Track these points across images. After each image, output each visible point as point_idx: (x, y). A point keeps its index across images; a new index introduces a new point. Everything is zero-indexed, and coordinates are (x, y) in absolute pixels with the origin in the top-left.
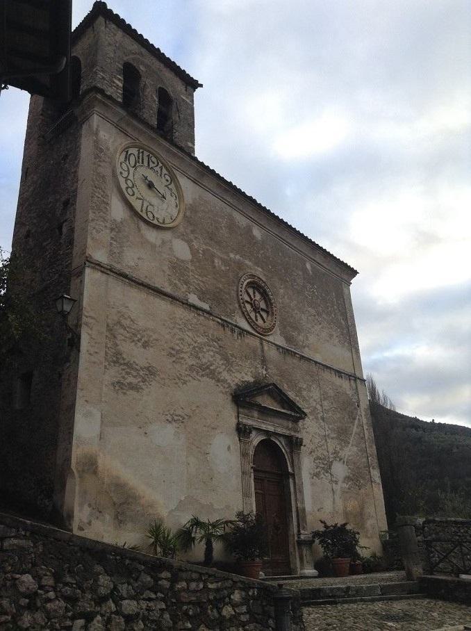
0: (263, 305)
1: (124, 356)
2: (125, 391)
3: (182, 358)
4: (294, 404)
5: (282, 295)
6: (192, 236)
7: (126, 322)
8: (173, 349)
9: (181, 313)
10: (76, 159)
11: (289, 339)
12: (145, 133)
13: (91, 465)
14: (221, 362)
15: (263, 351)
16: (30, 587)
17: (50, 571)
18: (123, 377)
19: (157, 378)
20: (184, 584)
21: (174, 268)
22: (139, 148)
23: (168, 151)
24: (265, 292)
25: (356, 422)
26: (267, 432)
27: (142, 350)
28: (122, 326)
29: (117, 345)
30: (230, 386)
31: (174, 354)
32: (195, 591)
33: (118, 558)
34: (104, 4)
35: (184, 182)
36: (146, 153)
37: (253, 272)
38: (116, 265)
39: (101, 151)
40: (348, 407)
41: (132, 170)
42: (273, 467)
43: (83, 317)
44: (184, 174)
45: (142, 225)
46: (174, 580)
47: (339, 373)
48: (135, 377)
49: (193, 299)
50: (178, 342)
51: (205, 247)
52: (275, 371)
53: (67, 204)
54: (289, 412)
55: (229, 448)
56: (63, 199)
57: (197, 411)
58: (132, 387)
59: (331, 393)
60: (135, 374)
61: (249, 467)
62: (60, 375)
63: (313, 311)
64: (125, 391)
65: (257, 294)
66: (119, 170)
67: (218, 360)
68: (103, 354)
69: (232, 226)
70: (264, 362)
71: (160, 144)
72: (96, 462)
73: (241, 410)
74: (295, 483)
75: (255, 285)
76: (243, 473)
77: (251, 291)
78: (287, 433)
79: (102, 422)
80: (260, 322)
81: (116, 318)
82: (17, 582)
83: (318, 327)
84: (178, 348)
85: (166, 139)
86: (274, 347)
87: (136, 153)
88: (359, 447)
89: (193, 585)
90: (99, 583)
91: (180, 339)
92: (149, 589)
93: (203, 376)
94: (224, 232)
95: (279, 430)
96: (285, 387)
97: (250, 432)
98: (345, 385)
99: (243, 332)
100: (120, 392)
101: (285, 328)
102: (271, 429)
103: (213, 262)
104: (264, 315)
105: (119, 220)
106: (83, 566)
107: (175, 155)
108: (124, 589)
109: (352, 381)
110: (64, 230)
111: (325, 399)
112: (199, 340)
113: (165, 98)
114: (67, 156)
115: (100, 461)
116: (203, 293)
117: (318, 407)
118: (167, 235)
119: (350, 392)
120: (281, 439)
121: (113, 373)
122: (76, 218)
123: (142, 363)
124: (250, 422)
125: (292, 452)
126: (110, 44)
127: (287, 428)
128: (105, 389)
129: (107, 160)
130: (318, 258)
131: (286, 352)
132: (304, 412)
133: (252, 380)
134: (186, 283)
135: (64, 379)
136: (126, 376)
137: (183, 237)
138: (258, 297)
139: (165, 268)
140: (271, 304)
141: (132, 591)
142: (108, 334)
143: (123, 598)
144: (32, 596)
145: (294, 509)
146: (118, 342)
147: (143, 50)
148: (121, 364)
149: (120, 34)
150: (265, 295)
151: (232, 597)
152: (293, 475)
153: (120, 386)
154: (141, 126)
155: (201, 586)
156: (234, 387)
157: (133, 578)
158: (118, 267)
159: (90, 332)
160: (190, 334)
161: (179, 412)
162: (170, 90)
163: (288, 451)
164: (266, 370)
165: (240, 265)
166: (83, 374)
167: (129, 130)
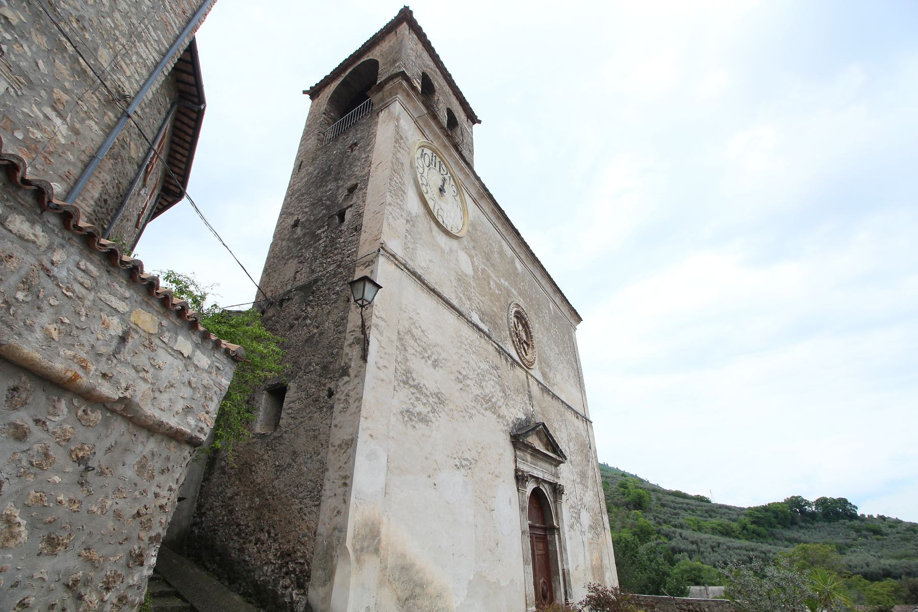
1: (414, 375)
2: (413, 423)
3: (468, 386)
6: (473, 252)
7: (417, 332)
10: (369, 145)
12: (439, 137)
13: (372, 538)
18: (413, 404)
19: (446, 409)
21: (460, 280)
22: (434, 151)
23: (457, 163)
24: (526, 323)
27: (432, 369)
28: (413, 336)
30: (508, 424)
31: (461, 379)
34: (411, 12)
36: (438, 159)
39: (402, 138)
41: (426, 169)
43: (374, 317)
45: (433, 225)
48: (424, 404)
49: (475, 318)
50: (464, 365)
53: (352, 190)
54: (551, 454)
56: (349, 184)
58: (424, 420)
62: (331, 394)
64: (413, 423)
68: (392, 369)
69: (501, 252)
72: (379, 532)
73: (518, 453)
75: (519, 316)
76: (523, 532)
83: (561, 366)
84: (464, 373)
91: (467, 362)
93: (486, 409)
100: (408, 425)
102: (540, 475)
105: (414, 214)
110: (348, 216)
113: (453, 122)
114: (356, 144)
115: (383, 530)
118: (454, 244)
121: (402, 398)
122: (367, 202)
126: (412, 49)
128: (393, 419)
134: (470, 299)
135: (339, 400)
136: (416, 403)
137: (465, 249)
139: (453, 278)
140: (532, 337)
142: (398, 344)
146: (408, 357)
158: (411, 264)
159: (380, 338)
160: (474, 357)
161: (466, 455)
165: (508, 293)
166: (368, 396)
167: (427, 132)
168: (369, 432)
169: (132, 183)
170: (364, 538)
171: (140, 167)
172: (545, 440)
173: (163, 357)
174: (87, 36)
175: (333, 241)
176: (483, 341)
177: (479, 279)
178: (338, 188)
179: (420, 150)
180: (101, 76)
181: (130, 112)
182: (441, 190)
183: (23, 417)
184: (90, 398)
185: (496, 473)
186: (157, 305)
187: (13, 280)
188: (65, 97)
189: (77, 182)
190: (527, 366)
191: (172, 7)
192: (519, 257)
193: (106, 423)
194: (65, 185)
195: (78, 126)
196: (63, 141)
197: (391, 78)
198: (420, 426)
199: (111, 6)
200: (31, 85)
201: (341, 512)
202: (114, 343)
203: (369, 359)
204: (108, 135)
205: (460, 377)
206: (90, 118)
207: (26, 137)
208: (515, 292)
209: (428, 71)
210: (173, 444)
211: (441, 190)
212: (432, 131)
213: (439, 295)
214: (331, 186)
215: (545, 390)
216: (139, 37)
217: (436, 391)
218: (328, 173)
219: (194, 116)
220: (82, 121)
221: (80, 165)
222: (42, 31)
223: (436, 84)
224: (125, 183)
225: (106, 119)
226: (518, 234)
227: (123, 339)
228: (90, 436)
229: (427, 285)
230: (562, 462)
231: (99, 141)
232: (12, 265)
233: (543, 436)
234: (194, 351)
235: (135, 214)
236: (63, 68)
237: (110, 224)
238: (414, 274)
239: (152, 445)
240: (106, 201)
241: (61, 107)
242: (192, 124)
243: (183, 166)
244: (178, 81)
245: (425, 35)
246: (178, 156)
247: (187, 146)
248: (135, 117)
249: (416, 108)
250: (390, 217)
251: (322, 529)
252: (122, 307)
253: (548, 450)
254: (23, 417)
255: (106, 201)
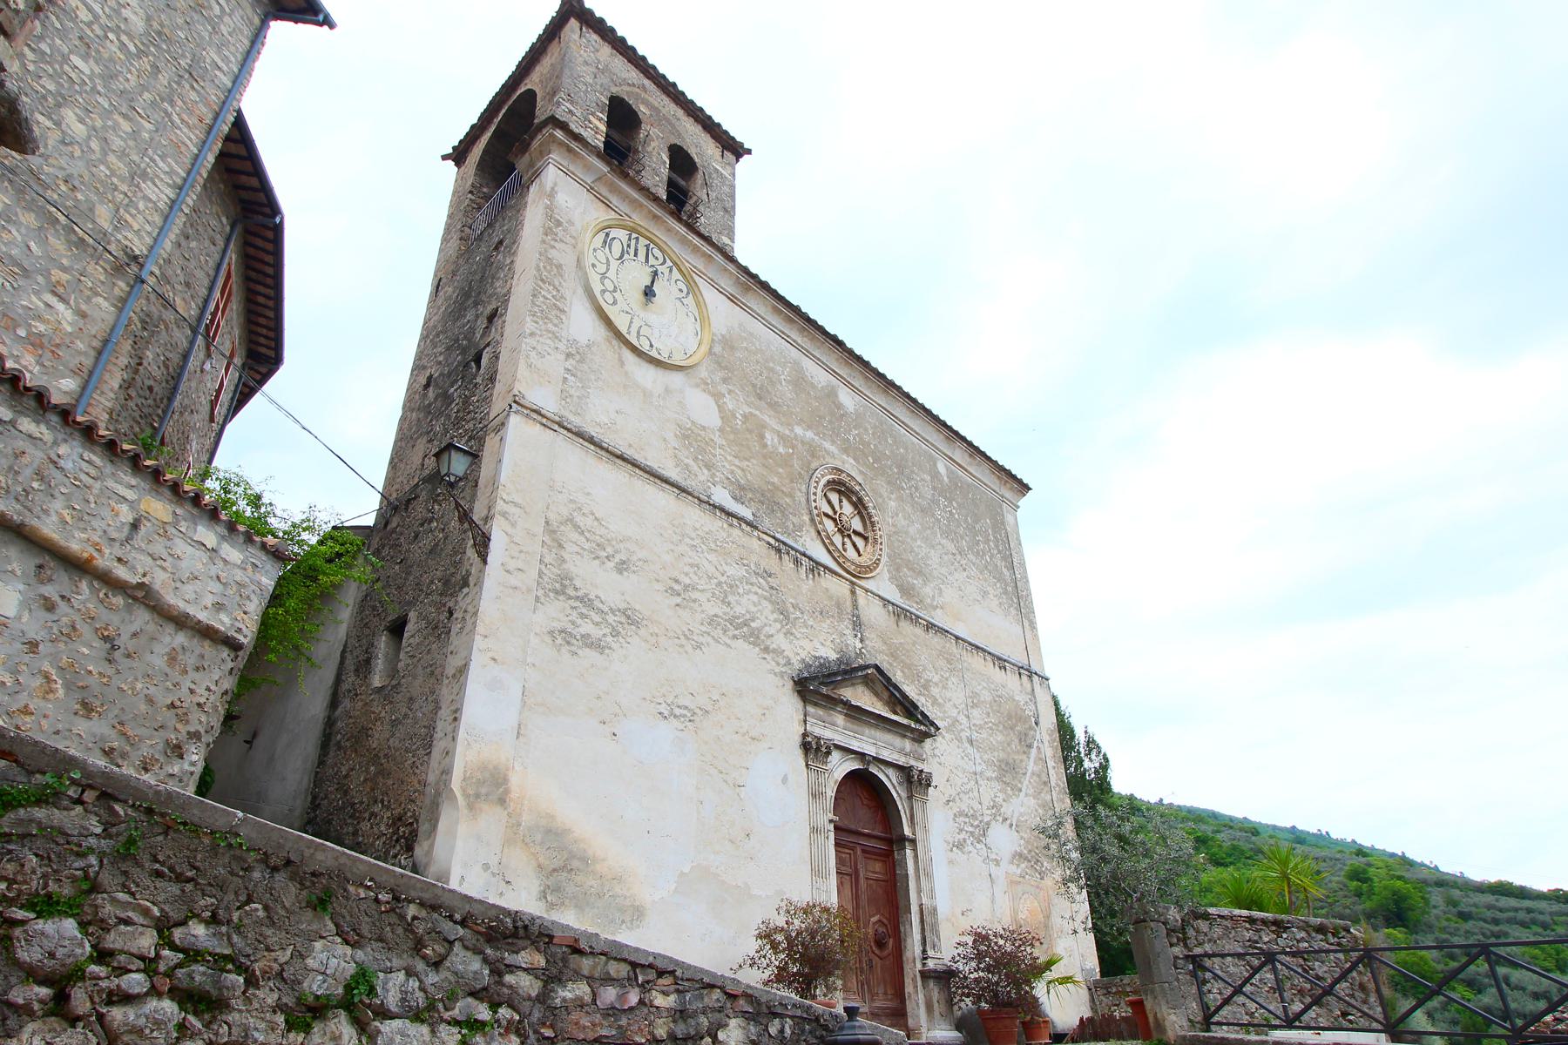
0: (857, 524)
1: (578, 583)
3: (694, 601)
4: (916, 707)
5: (889, 511)
6: (723, 388)
8: (677, 581)
9: (695, 516)
11: (905, 590)
12: (641, 205)
13: (493, 787)
14: (772, 617)
15: (855, 606)
16: (60, 953)
17: (146, 912)
18: (573, 623)
19: (642, 632)
20: (581, 990)
22: (632, 230)
24: (860, 500)
25: (1034, 751)
26: (861, 756)
27: (615, 575)
28: (577, 527)
29: (564, 561)
30: (789, 663)
31: (679, 591)
32: (612, 1012)
33: (384, 897)
35: (710, 296)
37: (839, 465)
38: (572, 418)
39: (559, 224)
40: (1018, 725)
41: (614, 264)
42: (871, 822)
44: (713, 284)
45: (628, 355)
46: (551, 978)
47: (1001, 662)
48: (597, 624)
49: (722, 496)
50: (687, 569)
51: (748, 410)
52: (879, 645)
53: (491, 318)
54: (905, 721)
55: (785, 780)
57: (721, 703)
59: (986, 696)
60: (597, 618)
61: (825, 818)
62: (451, 613)
63: (951, 547)
65: (845, 502)
66: (589, 260)
67: (767, 612)
69: (800, 382)
70: (857, 624)
71: (669, 230)
72: (506, 780)
73: (811, 709)
74: (916, 856)
75: (841, 487)
76: (814, 830)
77: (834, 497)
78: (902, 761)
79: (524, 703)
80: (851, 553)
81: (565, 512)
82: (18, 932)
84: (688, 581)
85: (680, 220)
86: (877, 601)
87: (625, 240)
88: (1041, 795)
89: (609, 995)
90: (310, 962)
92: (473, 994)
93: (735, 637)
94: (785, 391)
95: (886, 755)
96: (898, 677)
97: (828, 753)
98: (1011, 683)
99: (816, 566)
101: (898, 569)
102: (870, 750)
103: (762, 437)
104: (860, 542)
105: (583, 341)
106: (266, 908)
107: (696, 249)
108: (392, 988)
109: (1025, 678)
110: (484, 361)
111: (975, 706)
112: (731, 571)
113: (682, 162)
114: (501, 242)
115: (514, 780)
116: (742, 488)
117: (962, 719)
118: (676, 379)
119: (1021, 698)
120: (891, 772)
121: (555, 612)
123: (613, 599)
124: (827, 734)
125: (910, 797)
126: (586, 63)
127: (901, 751)
129: (568, 239)
130: (959, 455)
131: (901, 614)
132: (933, 724)
133: (833, 656)
134: (708, 467)
136: (579, 621)
137: (704, 385)
138: (848, 509)
139: (670, 436)
140: (873, 524)
141: (419, 995)
142: (547, 539)
143: (384, 1014)
144: (61, 982)
145: (914, 908)
146: (567, 556)
147: (647, 82)
148: (570, 598)
149: (606, 50)
150: (859, 506)
151: (721, 1035)
152: (913, 842)
153: (564, 637)
154: (635, 195)
155: (633, 998)
156: (798, 666)
157: (424, 957)
158: (575, 421)
159: (510, 530)
161: (685, 701)
162: (693, 152)
163: (904, 795)
164: (861, 641)
165: (813, 451)
167: (615, 200)
168: (490, 654)
169: (185, 357)
170: (481, 783)
171: (195, 331)
172: (886, 695)
173: (181, 547)
174: (80, 197)
175: (466, 401)
176: (736, 532)
177: (735, 431)
178: (477, 316)
179: (602, 235)
180: (103, 238)
181: (144, 275)
182: (649, 293)
183: (50, 591)
184: (106, 580)
185: (753, 733)
186: (167, 493)
187: (28, 472)
188: (65, 277)
189: (91, 373)
190: (856, 574)
191: (182, 120)
192: (848, 384)
193: (128, 606)
194: (79, 380)
195: (84, 307)
196: (69, 329)
197: (545, 123)
198: (589, 655)
199: (103, 149)
200: (26, 273)
201: (448, 753)
202: (126, 530)
203: (491, 558)
204: (121, 310)
205: (677, 587)
206: (97, 294)
207: (29, 334)
208: (832, 448)
209: (622, 92)
210: (207, 643)
211: (649, 293)
212: (625, 197)
213: (635, 464)
214: (470, 316)
215: (901, 614)
216: (144, 175)
217: (623, 606)
218: (466, 295)
219: (270, 235)
220: (88, 300)
221: (93, 353)
222: (28, 209)
223: (643, 110)
224: (175, 358)
225: (117, 291)
226: (840, 344)
227: (135, 526)
228: (115, 619)
229: (607, 450)
230: (927, 735)
231: (110, 319)
232: (25, 460)
233: (879, 688)
234: (219, 544)
235: (205, 402)
236: (57, 243)
237: (162, 419)
238: (579, 435)
239: (181, 639)
240: (150, 389)
241: (61, 290)
242: (270, 247)
243: (271, 314)
244: (237, 187)
245: (612, 30)
246: (261, 300)
247: (269, 281)
248: (152, 280)
249: (588, 168)
250: (533, 354)
251: (431, 778)
252: (130, 495)
253: (895, 713)
254: (50, 591)
255: (150, 389)
